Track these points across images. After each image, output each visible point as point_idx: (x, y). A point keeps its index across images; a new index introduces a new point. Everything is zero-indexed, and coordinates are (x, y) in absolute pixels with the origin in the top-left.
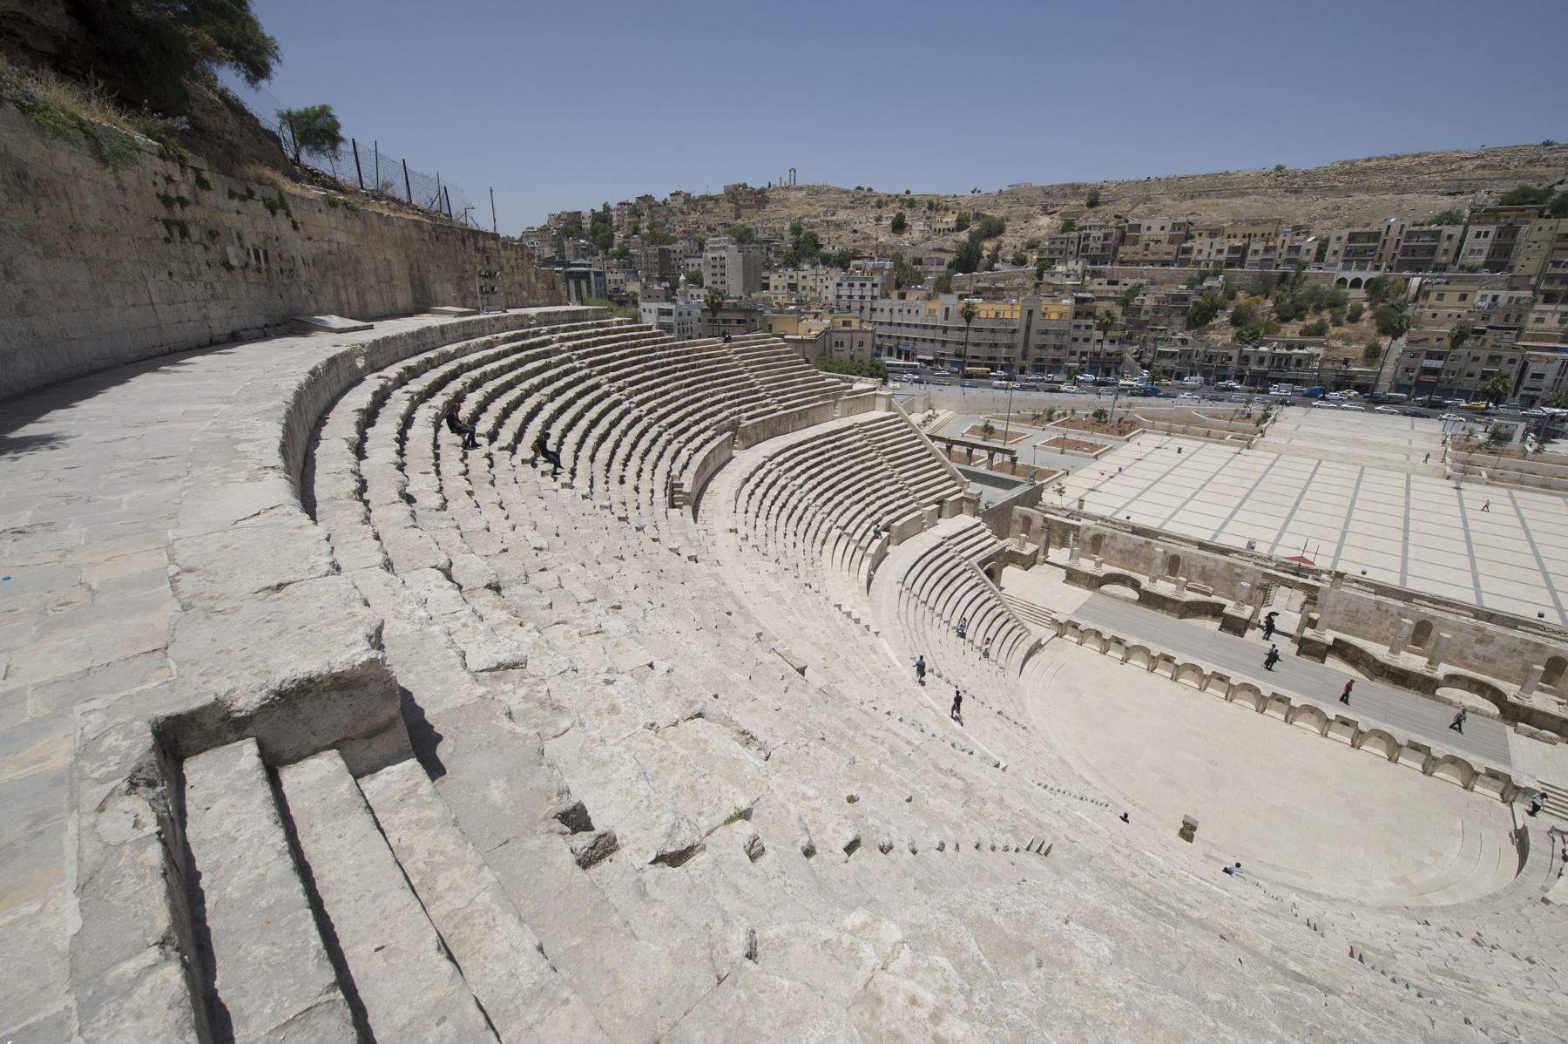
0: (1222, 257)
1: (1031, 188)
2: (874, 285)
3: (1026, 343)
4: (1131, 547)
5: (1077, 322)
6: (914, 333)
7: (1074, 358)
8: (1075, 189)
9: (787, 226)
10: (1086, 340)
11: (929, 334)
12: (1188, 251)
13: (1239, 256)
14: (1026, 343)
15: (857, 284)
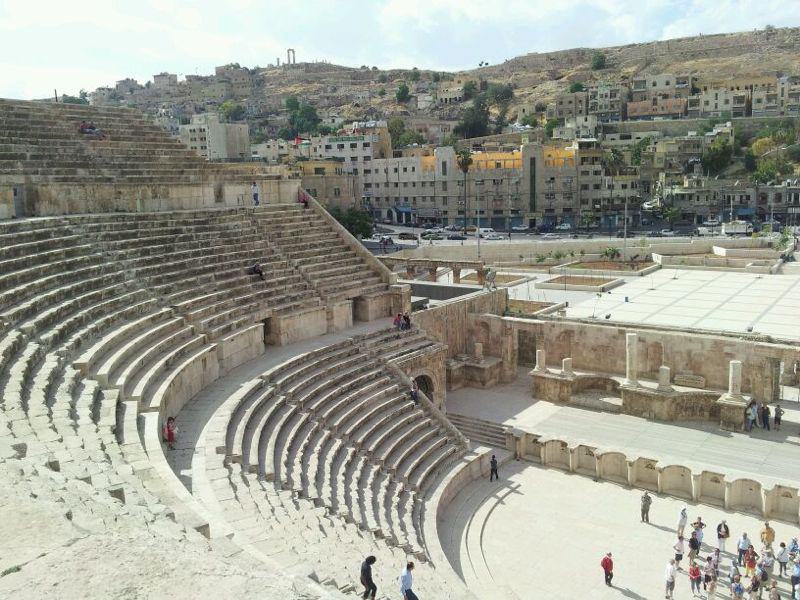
0: (729, 107)
1: (535, 56)
2: (366, 145)
3: (533, 194)
4: (604, 341)
5: (582, 168)
6: (411, 192)
7: (587, 207)
8: (580, 55)
9: (284, 102)
10: (597, 187)
11: (429, 191)
12: (694, 103)
13: (745, 108)
14: (533, 194)
15: (347, 145)
